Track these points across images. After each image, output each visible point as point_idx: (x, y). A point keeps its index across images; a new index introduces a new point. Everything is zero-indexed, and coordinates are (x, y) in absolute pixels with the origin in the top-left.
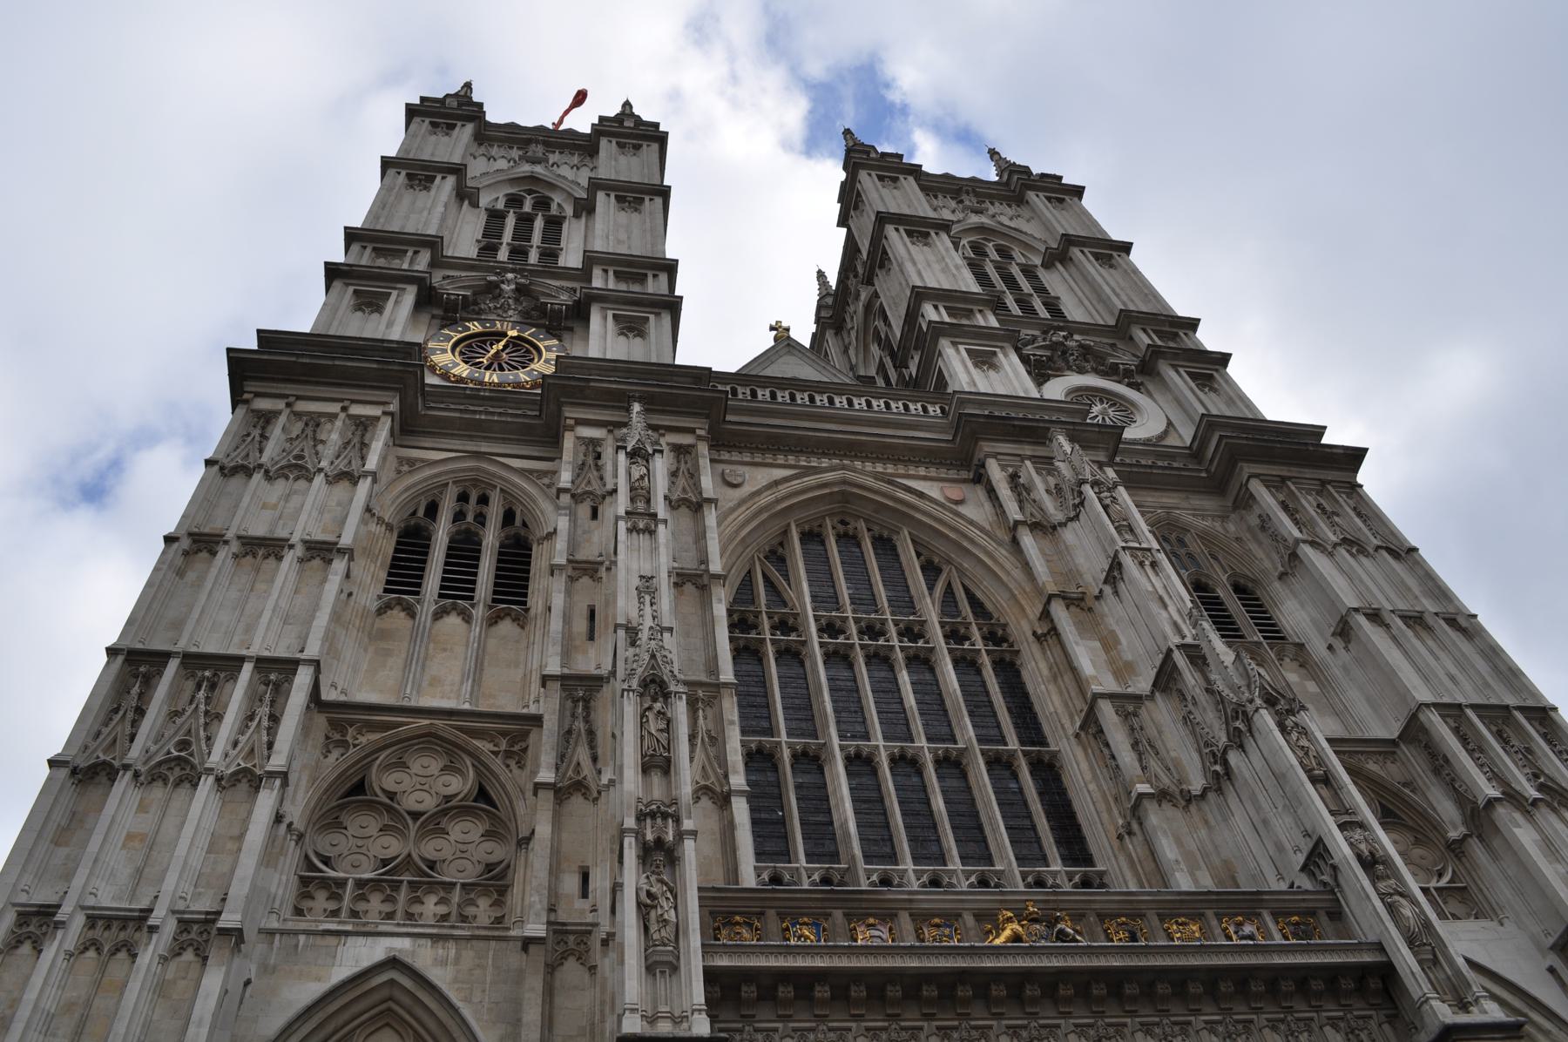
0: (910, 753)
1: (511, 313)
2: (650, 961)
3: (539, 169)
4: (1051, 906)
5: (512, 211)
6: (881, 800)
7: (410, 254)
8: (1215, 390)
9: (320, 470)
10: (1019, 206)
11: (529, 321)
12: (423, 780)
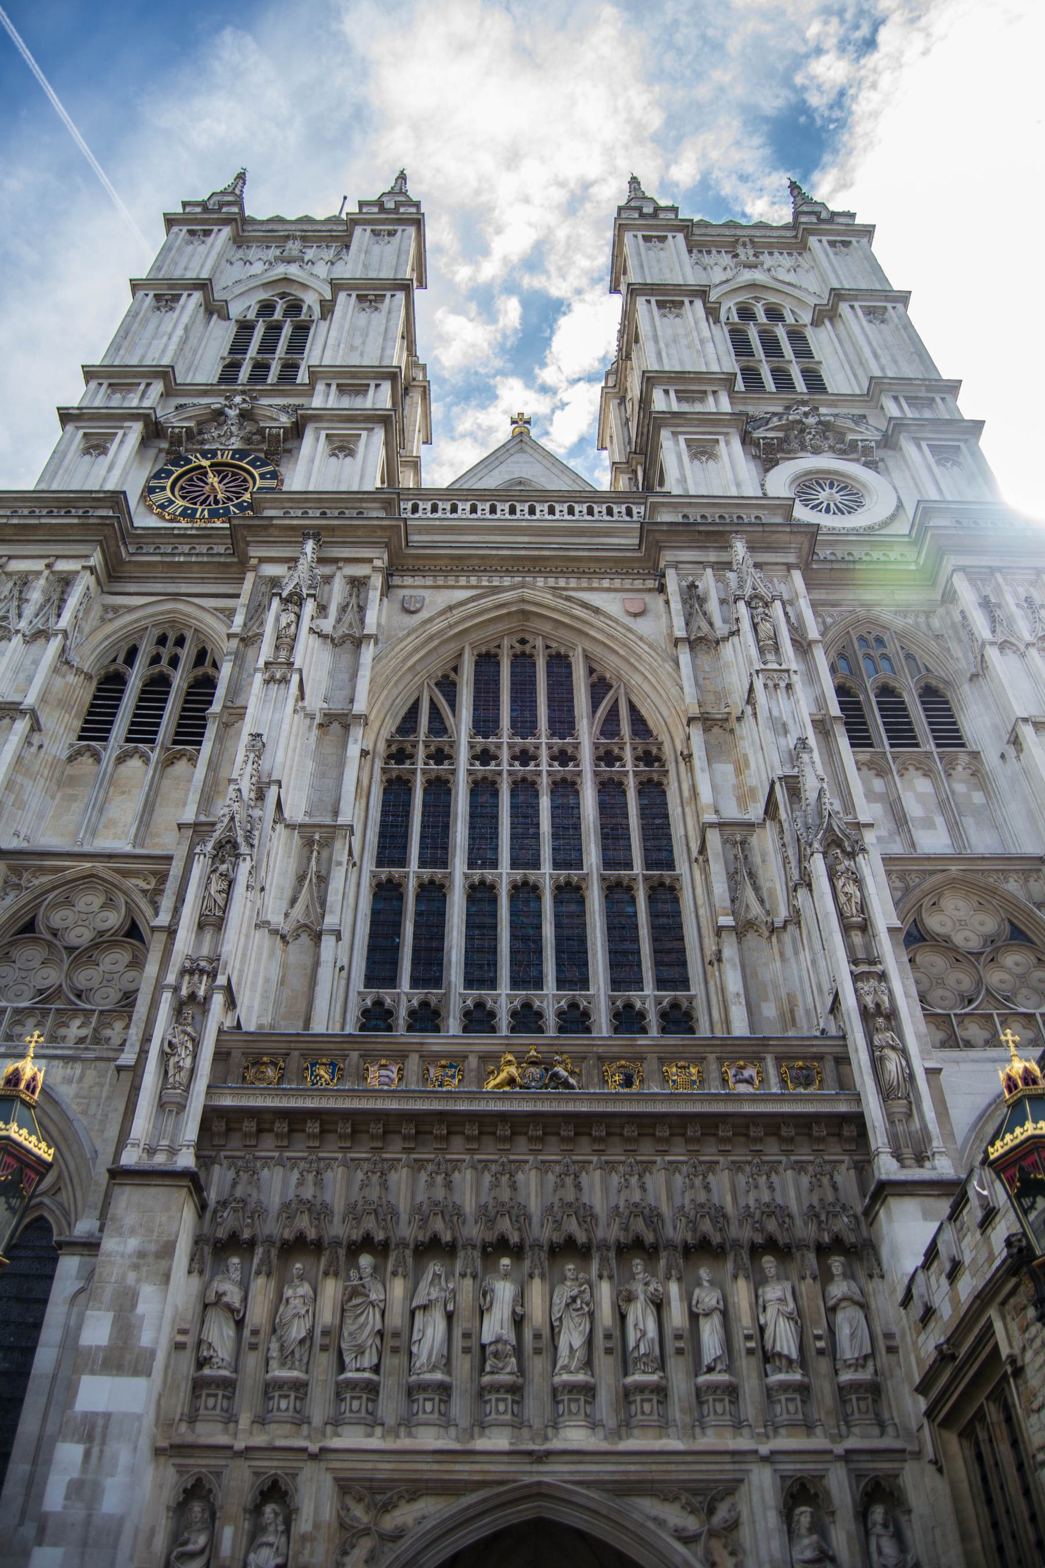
0: (532, 879)
1: (233, 440)
2: (164, 1100)
3: (293, 270)
4: (555, 1048)
6: (495, 927)
7: (142, 387)
8: (959, 464)
9: (18, 631)
10: (800, 254)
12: (84, 917)
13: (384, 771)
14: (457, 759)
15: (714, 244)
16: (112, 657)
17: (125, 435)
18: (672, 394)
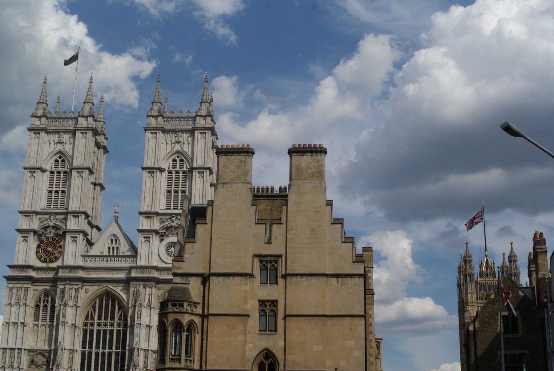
1: (52, 233)
5: (55, 170)
6: (98, 360)
7: (31, 217)
11: (55, 236)
13: (83, 329)
14: (94, 327)
15: (171, 131)
16: (36, 302)
17: (31, 236)
18: (144, 217)
